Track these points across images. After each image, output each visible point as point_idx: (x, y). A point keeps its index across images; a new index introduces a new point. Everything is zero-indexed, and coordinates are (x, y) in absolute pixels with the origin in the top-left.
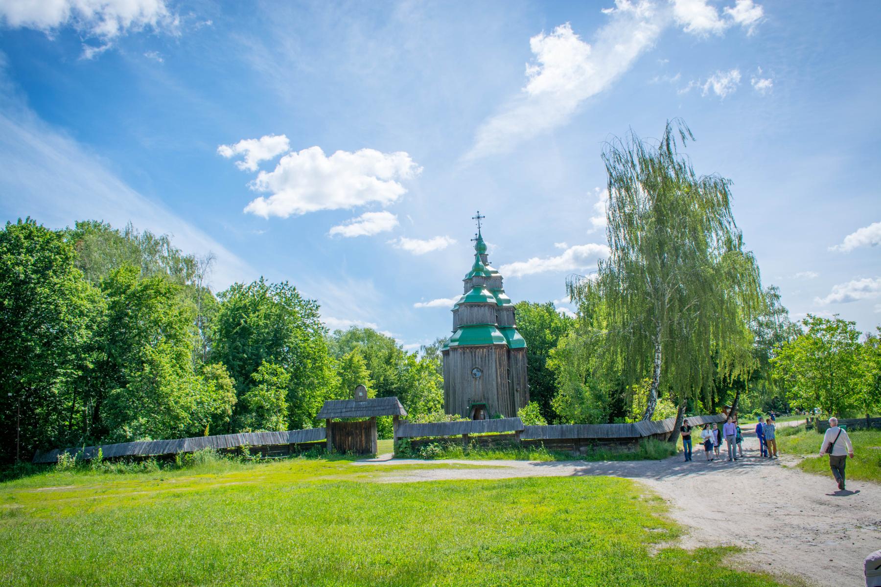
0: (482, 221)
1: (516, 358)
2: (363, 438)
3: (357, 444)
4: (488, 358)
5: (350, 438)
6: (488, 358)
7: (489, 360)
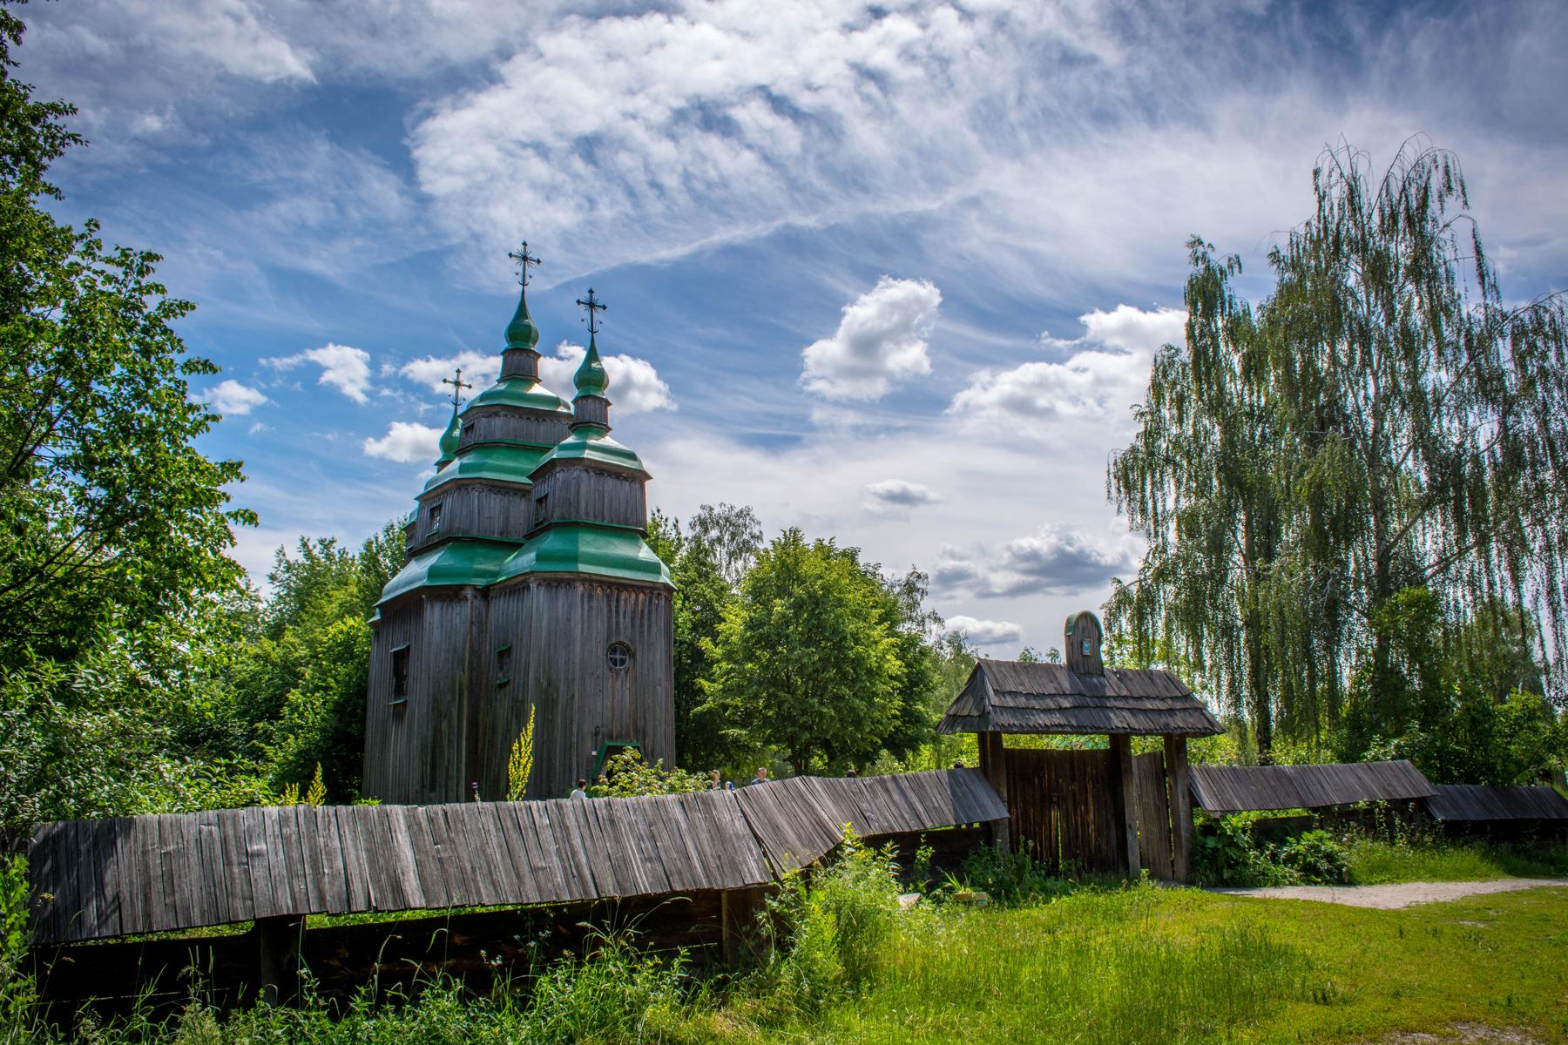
0: (532, 269)
4: (649, 619)
6: (649, 619)
7: (649, 626)
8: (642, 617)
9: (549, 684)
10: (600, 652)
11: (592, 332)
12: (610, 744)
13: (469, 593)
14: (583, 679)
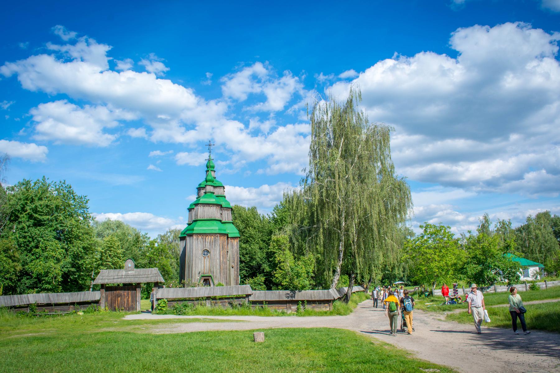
1: (233, 244)
2: (130, 299)
3: (124, 303)
4: (215, 243)
5: (119, 299)
7: (215, 245)
8: (213, 242)
10: (200, 252)
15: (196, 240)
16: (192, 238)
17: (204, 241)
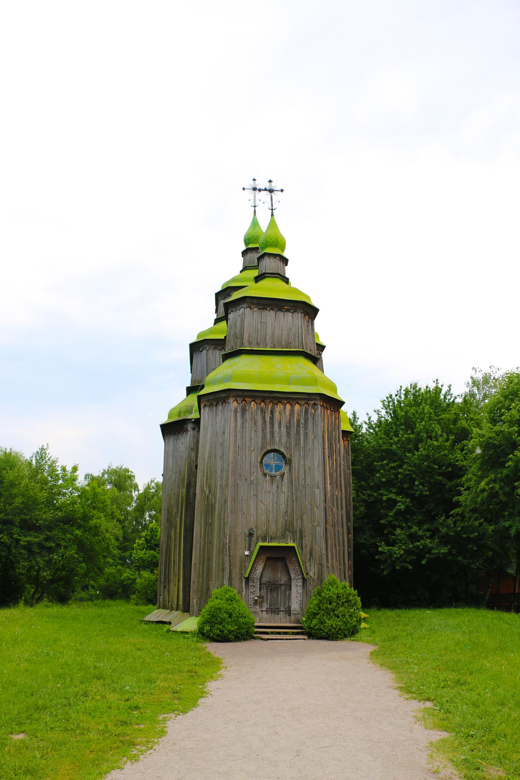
6: (306, 428)
7: (306, 434)
8: (298, 426)
9: (210, 492)
10: (255, 457)
11: (272, 210)
12: (261, 544)
13: (190, 426)
14: (236, 486)
15: (239, 415)
16: (220, 407)
17: (268, 419)
